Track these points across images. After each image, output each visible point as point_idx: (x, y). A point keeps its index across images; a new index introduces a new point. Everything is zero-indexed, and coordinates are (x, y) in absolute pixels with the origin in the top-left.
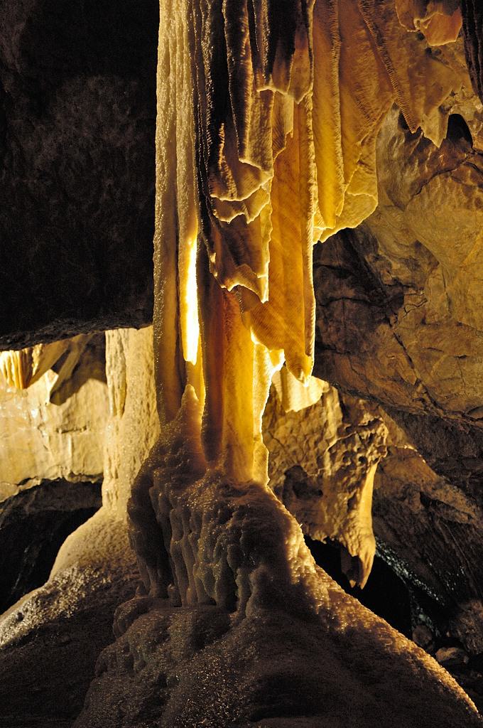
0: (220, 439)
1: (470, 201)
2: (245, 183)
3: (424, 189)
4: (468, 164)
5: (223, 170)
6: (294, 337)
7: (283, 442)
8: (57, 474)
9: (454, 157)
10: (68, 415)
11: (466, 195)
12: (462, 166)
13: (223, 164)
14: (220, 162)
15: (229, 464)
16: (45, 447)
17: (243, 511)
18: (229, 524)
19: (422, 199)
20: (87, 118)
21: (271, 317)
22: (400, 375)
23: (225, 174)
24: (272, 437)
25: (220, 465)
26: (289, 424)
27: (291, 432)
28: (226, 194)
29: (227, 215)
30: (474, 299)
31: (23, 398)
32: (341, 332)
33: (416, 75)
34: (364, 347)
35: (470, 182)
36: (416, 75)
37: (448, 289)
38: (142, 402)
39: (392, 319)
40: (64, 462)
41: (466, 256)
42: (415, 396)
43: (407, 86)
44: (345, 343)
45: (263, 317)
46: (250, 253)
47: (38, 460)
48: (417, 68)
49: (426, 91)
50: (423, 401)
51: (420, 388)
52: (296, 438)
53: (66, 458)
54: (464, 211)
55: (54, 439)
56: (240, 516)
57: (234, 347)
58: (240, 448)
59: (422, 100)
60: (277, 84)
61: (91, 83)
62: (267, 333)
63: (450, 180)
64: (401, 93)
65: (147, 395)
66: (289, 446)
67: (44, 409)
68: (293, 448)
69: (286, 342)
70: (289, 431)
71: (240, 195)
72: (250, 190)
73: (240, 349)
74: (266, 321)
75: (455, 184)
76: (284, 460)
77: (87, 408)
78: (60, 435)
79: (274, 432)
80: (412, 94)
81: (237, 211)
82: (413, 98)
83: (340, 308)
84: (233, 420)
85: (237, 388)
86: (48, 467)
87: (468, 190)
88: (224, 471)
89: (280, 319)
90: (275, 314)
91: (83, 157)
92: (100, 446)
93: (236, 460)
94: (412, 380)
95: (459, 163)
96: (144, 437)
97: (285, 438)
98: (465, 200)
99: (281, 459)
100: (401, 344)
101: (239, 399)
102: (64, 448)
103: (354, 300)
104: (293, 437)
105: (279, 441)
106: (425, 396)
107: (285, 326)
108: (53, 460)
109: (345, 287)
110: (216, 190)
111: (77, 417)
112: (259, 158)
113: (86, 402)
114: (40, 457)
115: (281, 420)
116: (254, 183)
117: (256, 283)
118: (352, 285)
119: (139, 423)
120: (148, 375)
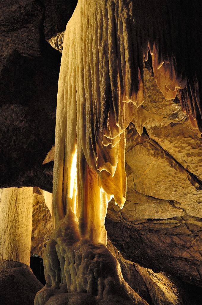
0: (87, 227)
1: (149, 153)
2: (114, 133)
3: (133, 149)
4: (148, 142)
5: (108, 127)
6: (118, 191)
7: (48, 229)
9: (143, 140)
11: (148, 151)
12: (146, 143)
13: (108, 125)
14: (108, 124)
15: (91, 236)
17: (100, 255)
18: (95, 260)
19: (132, 152)
20: (9, 117)
21: (109, 183)
22: (113, 208)
23: (109, 129)
24: (45, 228)
25: (87, 236)
26: (51, 223)
27: (52, 226)
28: (109, 136)
29: (106, 144)
30: (146, 185)
33: (139, 112)
35: (149, 148)
36: (139, 112)
37: (135, 181)
38: (6, 214)
41: (145, 171)
42: (118, 215)
43: (137, 115)
45: (106, 183)
46: (110, 159)
48: (139, 110)
49: (142, 117)
50: (120, 217)
51: (120, 213)
52: (53, 229)
54: (147, 156)
56: (99, 257)
57: (94, 193)
58: (95, 230)
59: (141, 120)
60: (132, 100)
61: (12, 107)
62: (107, 188)
63: (142, 146)
64: (136, 117)
65: (9, 211)
66: (50, 231)
68: (51, 232)
69: (114, 192)
70: (51, 226)
71: (112, 137)
72: (116, 136)
73: (95, 194)
74: (107, 184)
75: (144, 148)
76: (48, 235)
79: (46, 226)
80: (138, 118)
81: (109, 143)
82: (139, 119)
84: (93, 220)
85: (95, 208)
87: (148, 150)
88: (89, 239)
89: (112, 184)
90: (110, 182)
91: (6, 129)
93: (94, 235)
94: (117, 210)
95: (145, 142)
96: (6, 226)
97: (49, 228)
98: (147, 153)
99: (47, 235)
101: (95, 212)
104: (52, 228)
105: (47, 229)
106: (121, 216)
107: (114, 187)
110: (106, 134)
112: (121, 124)
115: (48, 222)
116: (117, 133)
117: (110, 169)
119: (5, 221)
120: (9, 205)
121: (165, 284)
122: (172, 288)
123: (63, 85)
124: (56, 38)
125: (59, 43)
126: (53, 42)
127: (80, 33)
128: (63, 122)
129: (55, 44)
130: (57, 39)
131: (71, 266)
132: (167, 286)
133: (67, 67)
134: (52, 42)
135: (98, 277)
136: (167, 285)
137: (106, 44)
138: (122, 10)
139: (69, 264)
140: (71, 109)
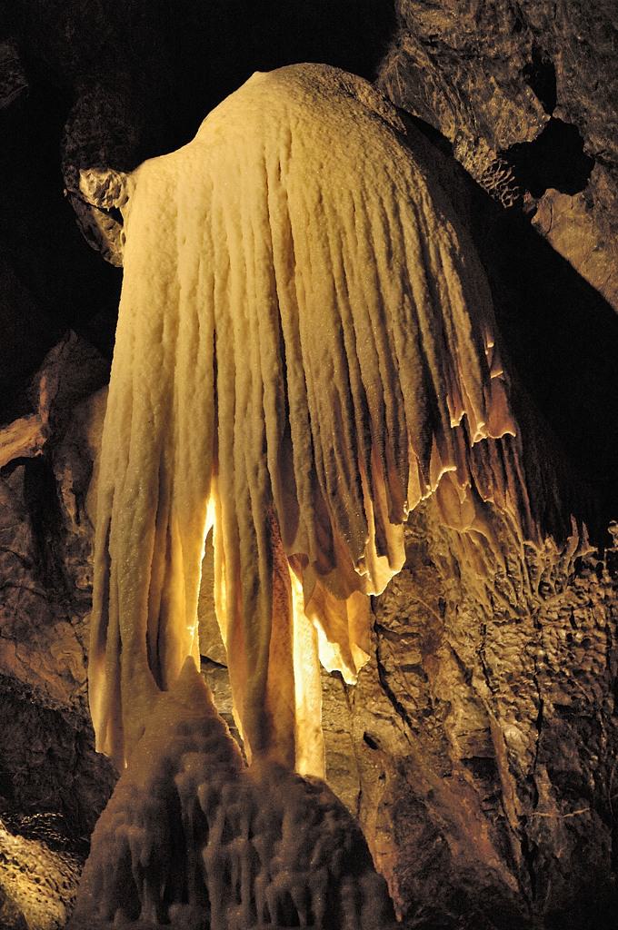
22: (70, 672)
25: (279, 754)
32: (11, 618)
34: (36, 638)
39: (75, 620)
44: (13, 628)
83: (16, 595)
94: (82, 678)
100: (81, 643)
103: (32, 592)
109: (27, 578)
118: (35, 577)
121: (37, 881)
122: (61, 887)
123: (158, 302)
124: (104, 177)
125: (110, 192)
126: (92, 182)
127: (259, 207)
128: (161, 400)
129: (99, 188)
130: (108, 181)
131: (240, 842)
132: (44, 885)
133: (172, 262)
134: (89, 183)
135: (342, 875)
136: (43, 881)
137: (404, 275)
138: (436, 227)
139: (227, 837)
140: (198, 377)
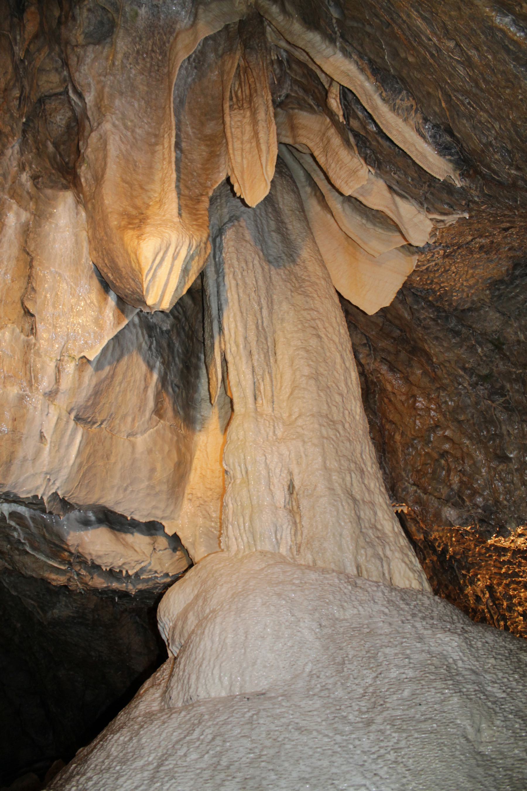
8: (37, 488)
10: (97, 393)
16: (41, 432)
31: (23, 337)
40: (59, 471)
47: (20, 454)
53: (65, 464)
55: (63, 423)
67: (70, 368)
77: (119, 392)
78: (72, 423)
86: (31, 471)
92: (113, 459)
102: (68, 446)
108: (46, 462)
111: (103, 401)
113: (121, 383)
114: (28, 448)
